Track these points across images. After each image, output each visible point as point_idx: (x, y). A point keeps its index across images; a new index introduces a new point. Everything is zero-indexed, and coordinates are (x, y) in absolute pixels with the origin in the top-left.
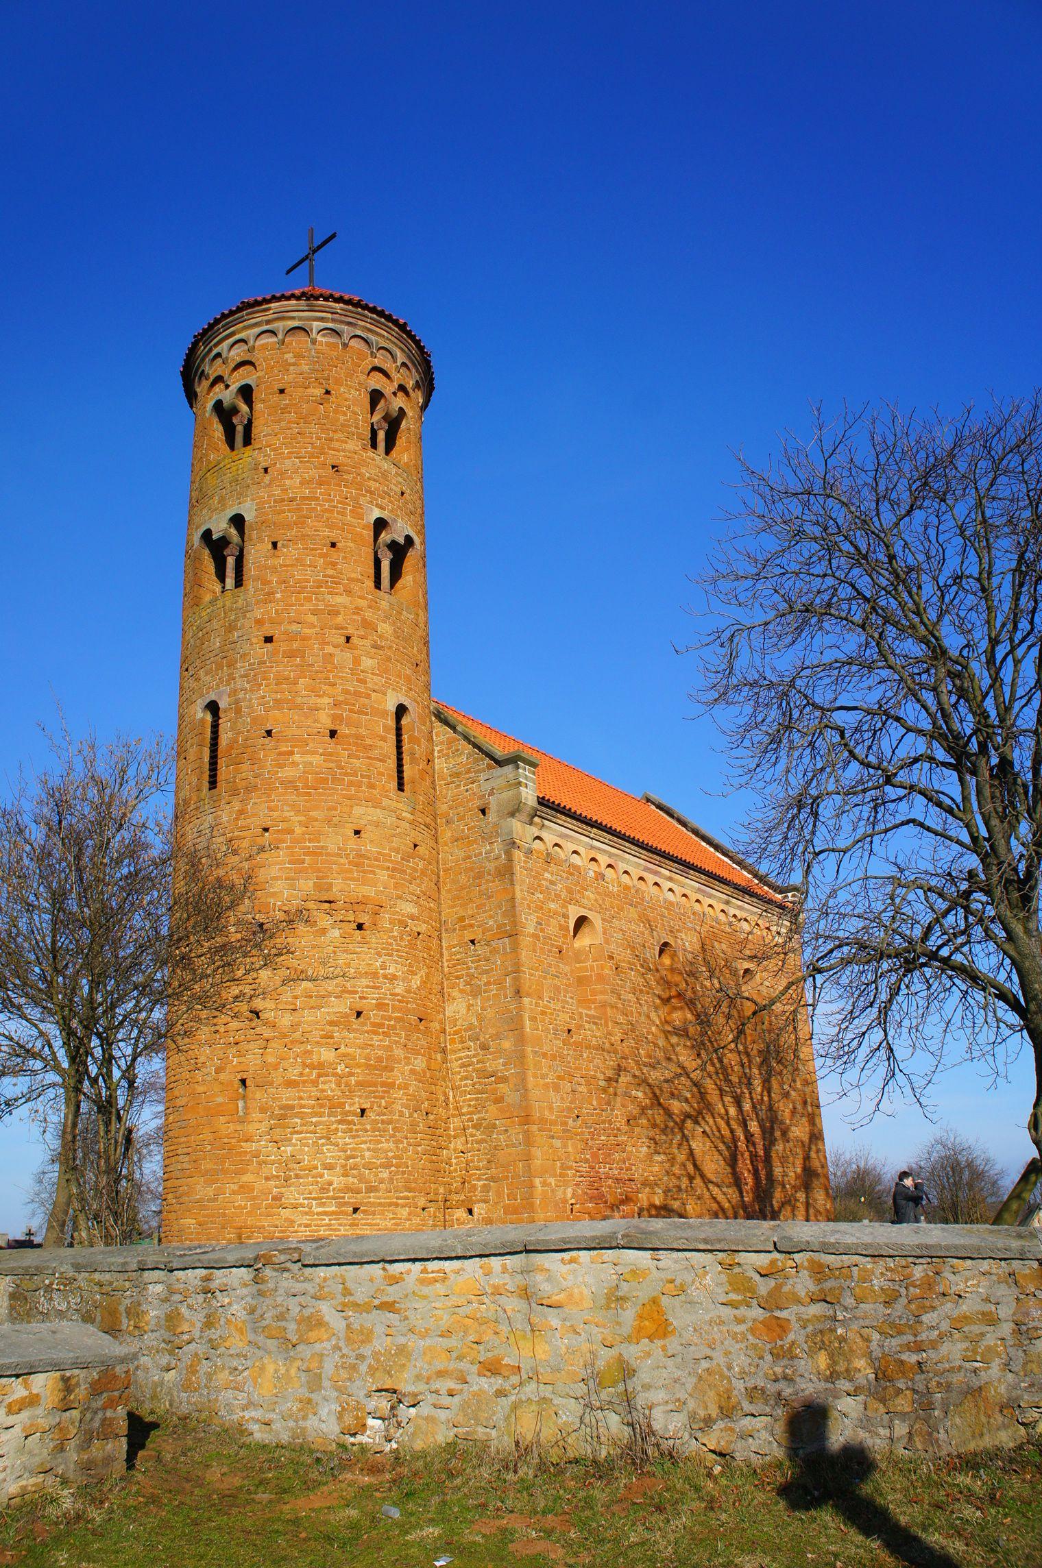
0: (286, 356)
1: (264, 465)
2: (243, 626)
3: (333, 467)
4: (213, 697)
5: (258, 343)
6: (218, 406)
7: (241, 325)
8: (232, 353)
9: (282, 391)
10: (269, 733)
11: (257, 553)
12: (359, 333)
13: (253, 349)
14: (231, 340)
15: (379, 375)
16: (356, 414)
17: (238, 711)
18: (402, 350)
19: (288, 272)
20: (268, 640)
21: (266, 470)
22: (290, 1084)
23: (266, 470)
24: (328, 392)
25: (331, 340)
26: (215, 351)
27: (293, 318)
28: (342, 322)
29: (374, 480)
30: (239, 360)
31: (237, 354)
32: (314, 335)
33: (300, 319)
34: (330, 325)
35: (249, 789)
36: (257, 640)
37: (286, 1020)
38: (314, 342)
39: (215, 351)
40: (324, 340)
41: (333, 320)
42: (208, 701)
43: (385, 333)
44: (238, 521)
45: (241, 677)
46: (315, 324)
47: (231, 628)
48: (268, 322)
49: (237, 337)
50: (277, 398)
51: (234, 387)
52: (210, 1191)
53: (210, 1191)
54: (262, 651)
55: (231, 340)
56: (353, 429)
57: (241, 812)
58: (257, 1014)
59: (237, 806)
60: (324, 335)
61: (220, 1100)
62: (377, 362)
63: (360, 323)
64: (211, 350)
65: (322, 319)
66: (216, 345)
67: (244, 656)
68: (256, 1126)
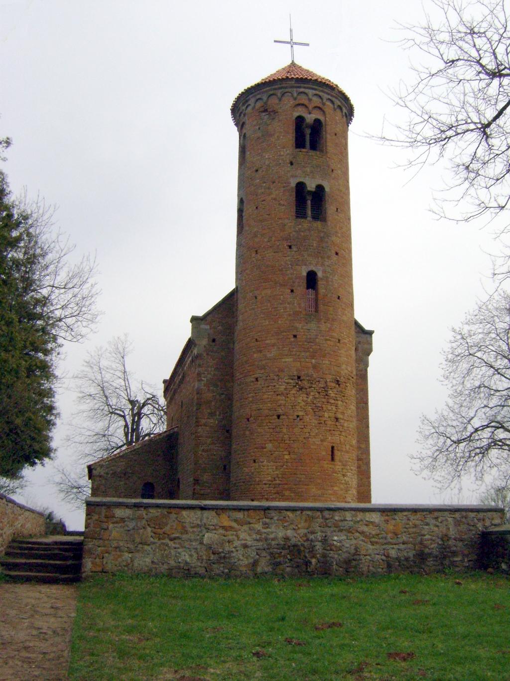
1: (333, 168)
2: (327, 242)
4: (314, 269)
6: (300, 120)
7: (321, 89)
10: (339, 298)
11: (330, 209)
17: (327, 281)
20: (337, 254)
21: (332, 170)
22: (347, 452)
23: (332, 170)
26: (302, 90)
27: (339, 100)
30: (316, 105)
31: (316, 101)
35: (333, 320)
36: (333, 252)
37: (346, 425)
39: (302, 90)
42: (310, 269)
44: (320, 188)
45: (328, 266)
47: (321, 240)
48: (332, 96)
49: (317, 92)
50: (334, 137)
52: (319, 492)
53: (319, 492)
54: (335, 258)
55: (314, 92)
57: (330, 329)
58: (337, 419)
59: (329, 325)
61: (324, 453)
66: (304, 88)
67: (329, 257)
68: (339, 467)
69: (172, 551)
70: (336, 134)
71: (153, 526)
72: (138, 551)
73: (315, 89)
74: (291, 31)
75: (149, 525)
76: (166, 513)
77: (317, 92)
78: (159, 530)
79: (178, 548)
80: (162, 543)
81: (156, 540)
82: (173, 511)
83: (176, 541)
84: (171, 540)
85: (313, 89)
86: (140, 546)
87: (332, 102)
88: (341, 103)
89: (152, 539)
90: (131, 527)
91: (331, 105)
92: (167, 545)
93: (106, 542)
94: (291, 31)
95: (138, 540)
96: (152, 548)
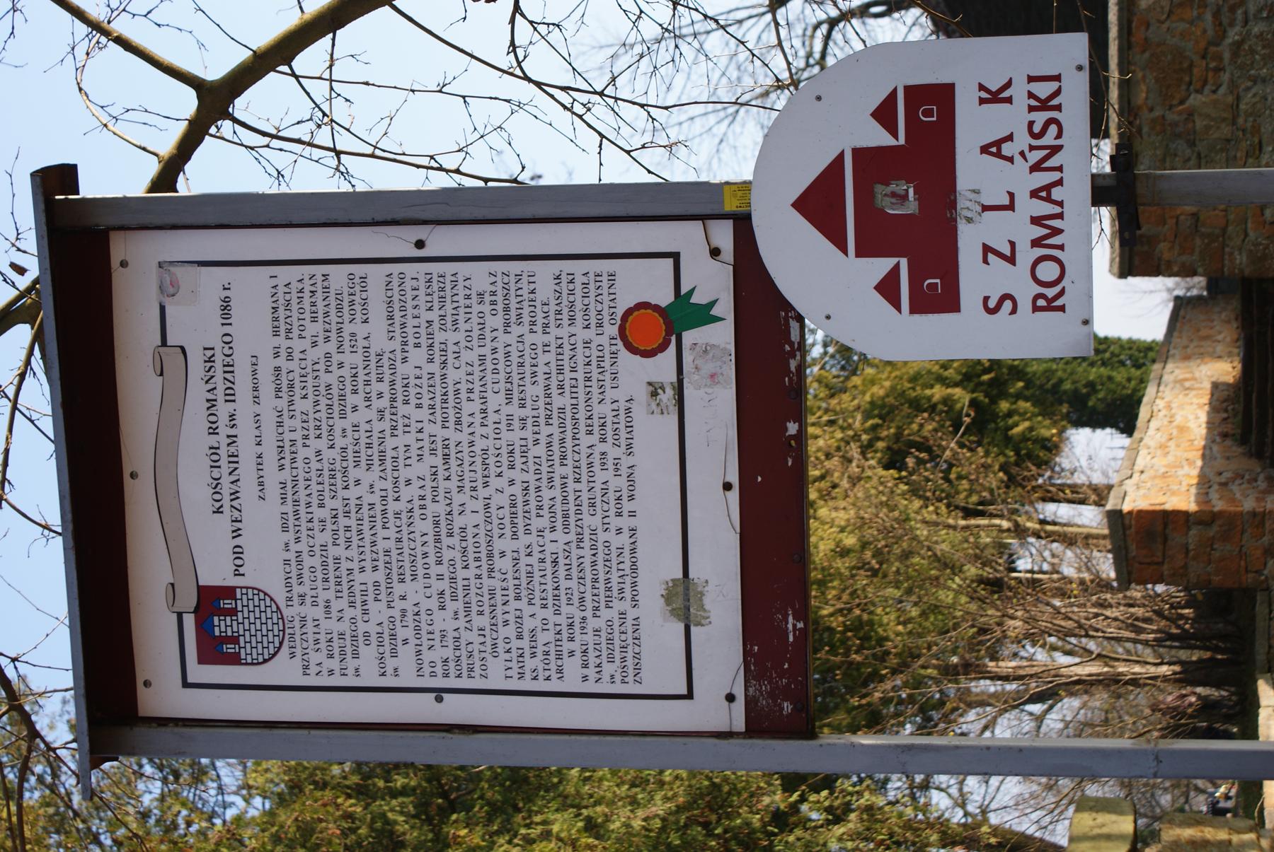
69: (1256, 30)
71: (1184, 87)
72: (1256, 130)
75: (1182, 102)
76: (1147, 55)
78: (1195, 71)
79: (1246, 13)
80: (1235, 55)
81: (1225, 77)
82: (1139, 35)
83: (1225, 21)
84: (1224, 35)
86: (1241, 121)
89: (1222, 91)
90: (1188, 151)
92: (1238, 45)
93: (1232, 217)
95: (1226, 130)
96: (1248, 89)
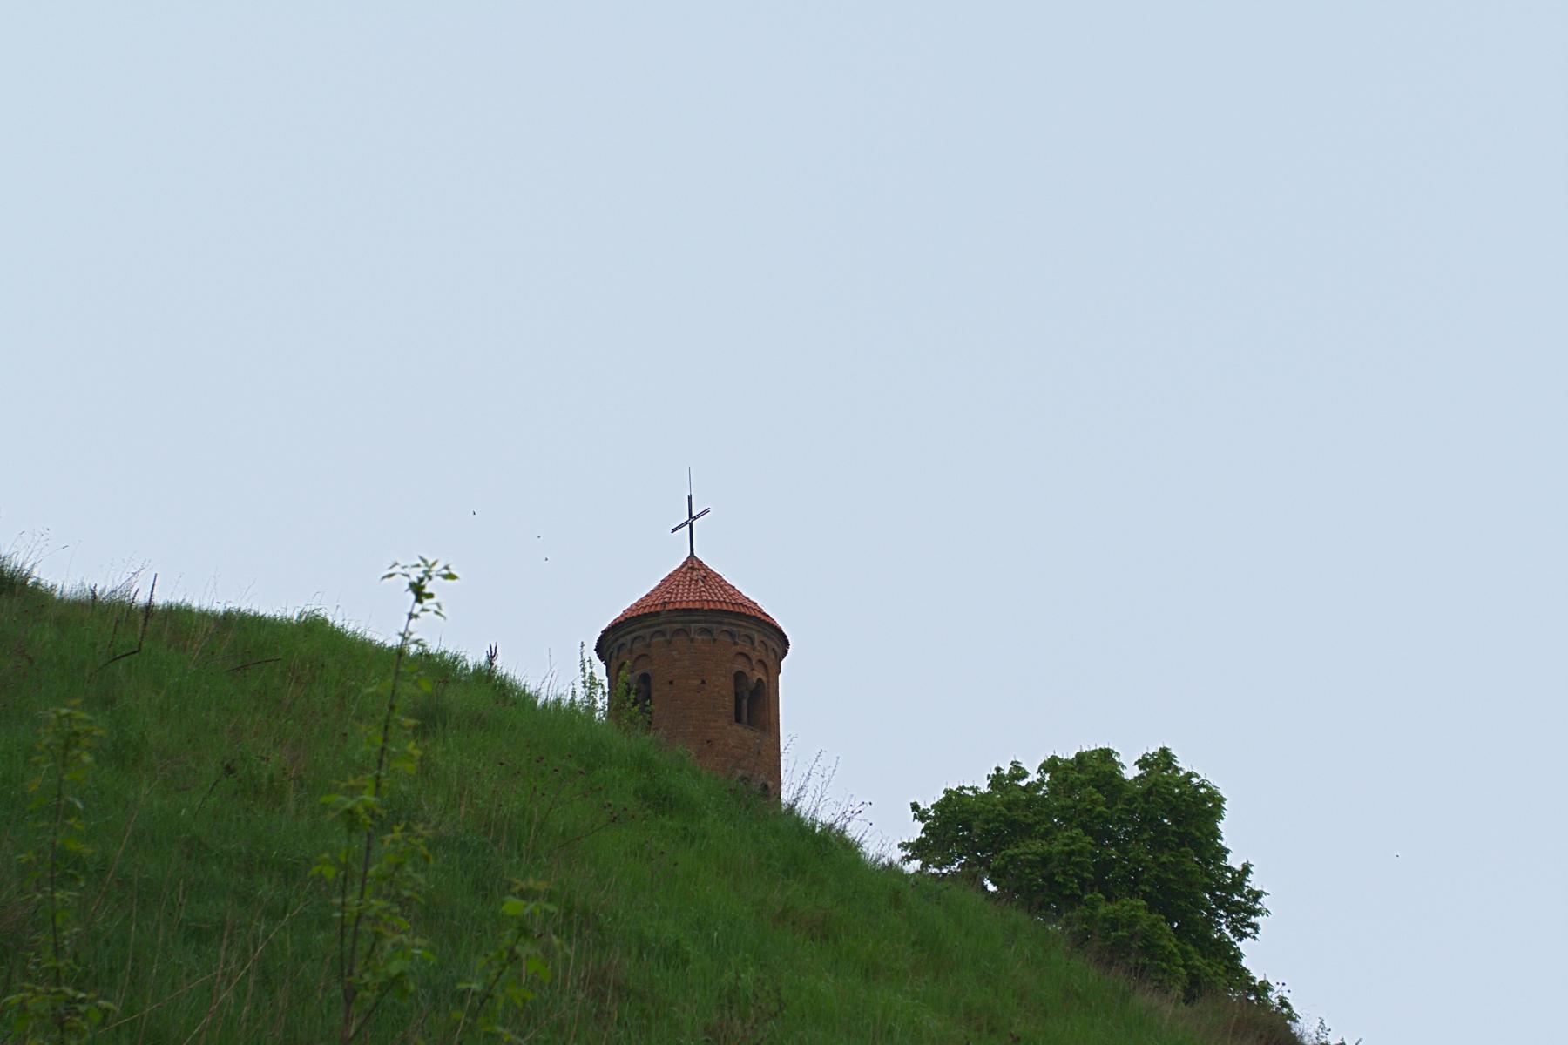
0: (674, 653)
3: (708, 742)
5: (655, 640)
8: (636, 646)
9: (671, 683)
12: (725, 628)
13: (649, 646)
14: (634, 635)
15: (742, 660)
16: (722, 696)
18: (759, 632)
19: (674, 530)
24: (703, 682)
25: (705, 637)
26: (620, 642)
27: (676, 622)
28: (711, 622)
29: (737, 748)
30: (639, 652)
32: (692, 636)
33: (682, 622)
34: (704, 625)
38: (692, 640)
39: (620, 642)
40: (699, 638)
41: (706, 622)
43: (744, 623)
46: (693, 625)
48: (659, 625)
49: (637, 634)
51: (638, 673)
55: (634, 635)
56: (722, 710)
60: (700, 634)
62: (738, 649)
63: (726, 620)
64: (617, 639)
65: (698, 622)
66: (623, 636)
70: (671, 683)
73: (634, 631)
74: (690, 498)
77: (637, 634)
85: (630, 633)
87: (662, 633)
88: (682, 622)
91: (662, 639)
94: (690, 498)
